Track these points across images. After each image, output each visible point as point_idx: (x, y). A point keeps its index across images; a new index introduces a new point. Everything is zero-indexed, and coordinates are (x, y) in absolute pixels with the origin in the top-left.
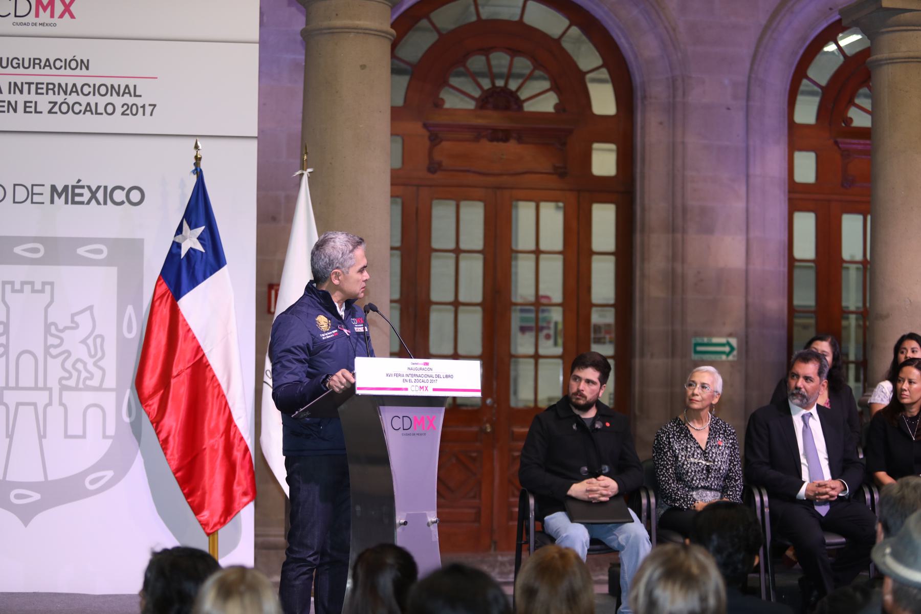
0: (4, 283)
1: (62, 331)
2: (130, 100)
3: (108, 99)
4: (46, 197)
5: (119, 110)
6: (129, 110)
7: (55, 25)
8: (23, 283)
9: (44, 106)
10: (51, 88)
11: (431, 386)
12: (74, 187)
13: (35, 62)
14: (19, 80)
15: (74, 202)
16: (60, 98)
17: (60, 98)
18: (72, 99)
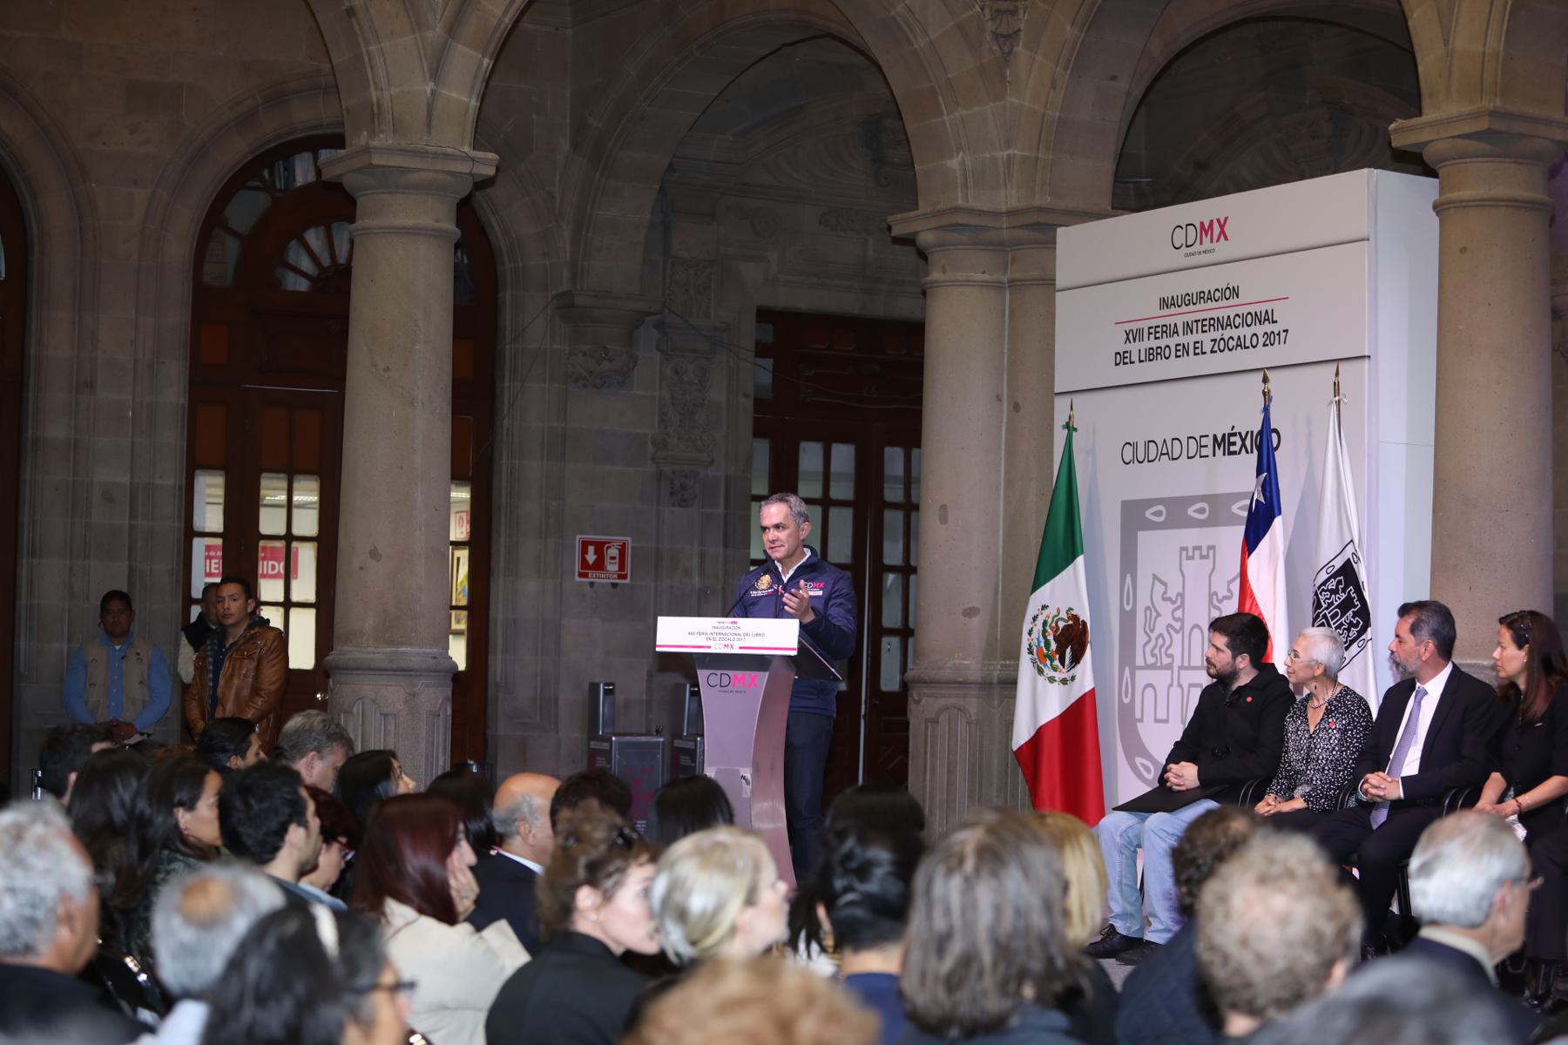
0: (1182, 549)
1: (1220, 601)
2: (1268, 327)
3: (1253, 329)
4: (1207, 451)
5: (1261, 340)
6: (1270, 339)
7: (1213, 251)
8: (1195, 548)
9: (1207, 346)
10: (1217, 323)
11: (737, 644)
12: (1231, 435)
13: (1204, 297)
14: (1190, 318)
15: (1231, 453)
16: (1217, 335)
17: (1217, 335)
18: (1228, 332)
